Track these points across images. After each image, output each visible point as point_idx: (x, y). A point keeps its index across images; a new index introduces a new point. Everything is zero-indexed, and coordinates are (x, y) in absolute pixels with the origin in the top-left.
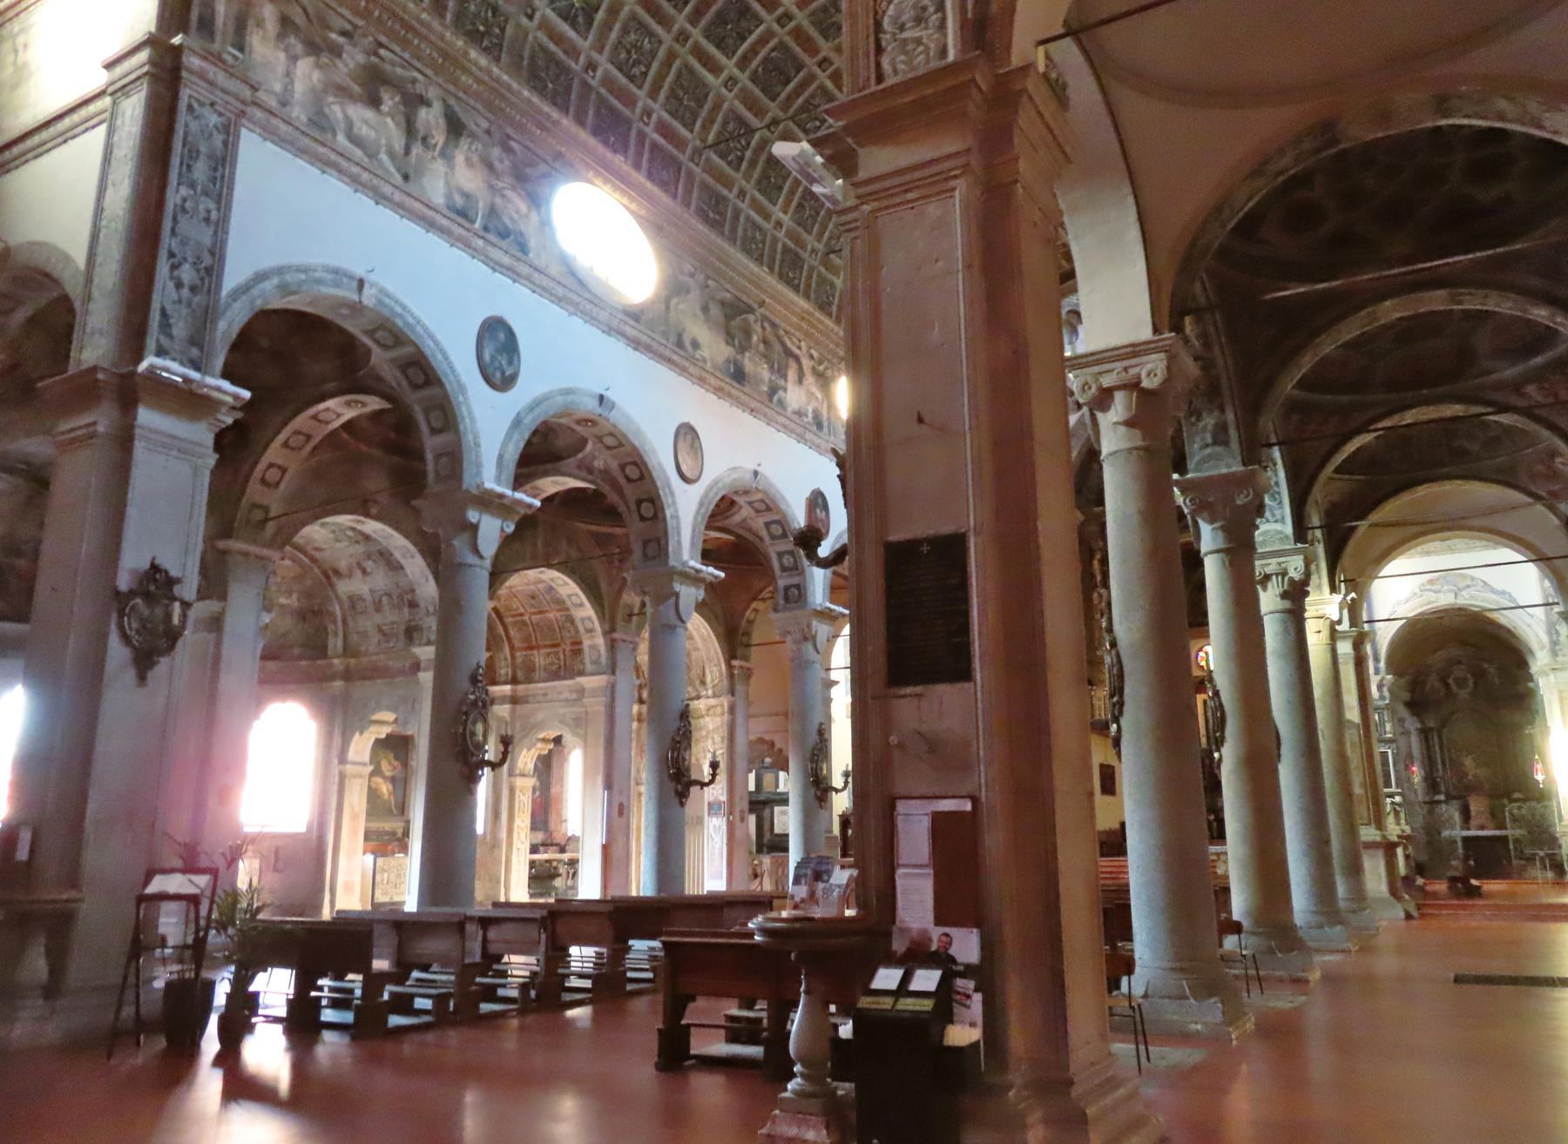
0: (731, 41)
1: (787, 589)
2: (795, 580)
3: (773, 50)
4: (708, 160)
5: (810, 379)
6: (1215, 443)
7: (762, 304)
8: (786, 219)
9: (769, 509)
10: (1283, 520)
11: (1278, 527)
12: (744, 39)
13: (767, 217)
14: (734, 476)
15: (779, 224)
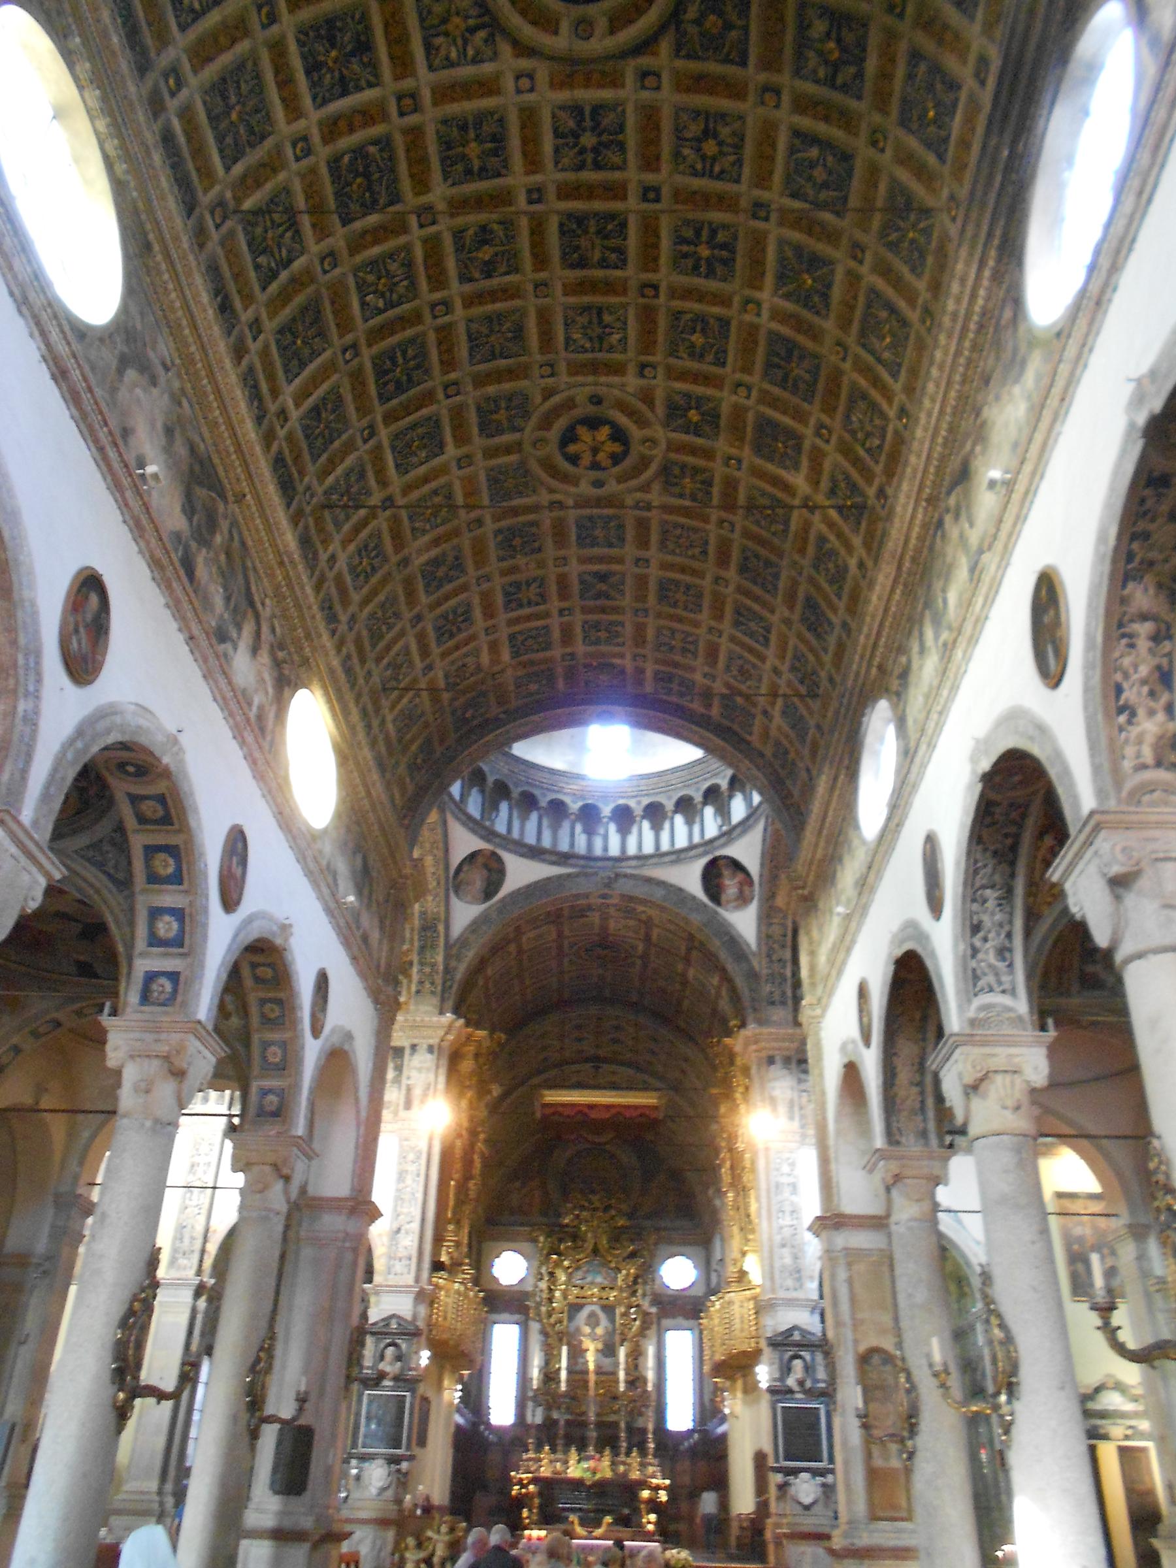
0: (328, 79)
1: (151, 977)
2: (170, 965)
3: (375, 142)
4: (231, 234)
5: (264, 658)
6: (1159, 764)
7: (240, 498)
8: (295, 414)
9: (166, 820)
10: (1013, 992)
11: (1006, 1000)
12: (345, 93)
13: (275, 393)
14: (142, 722)
15: (283, 414)
